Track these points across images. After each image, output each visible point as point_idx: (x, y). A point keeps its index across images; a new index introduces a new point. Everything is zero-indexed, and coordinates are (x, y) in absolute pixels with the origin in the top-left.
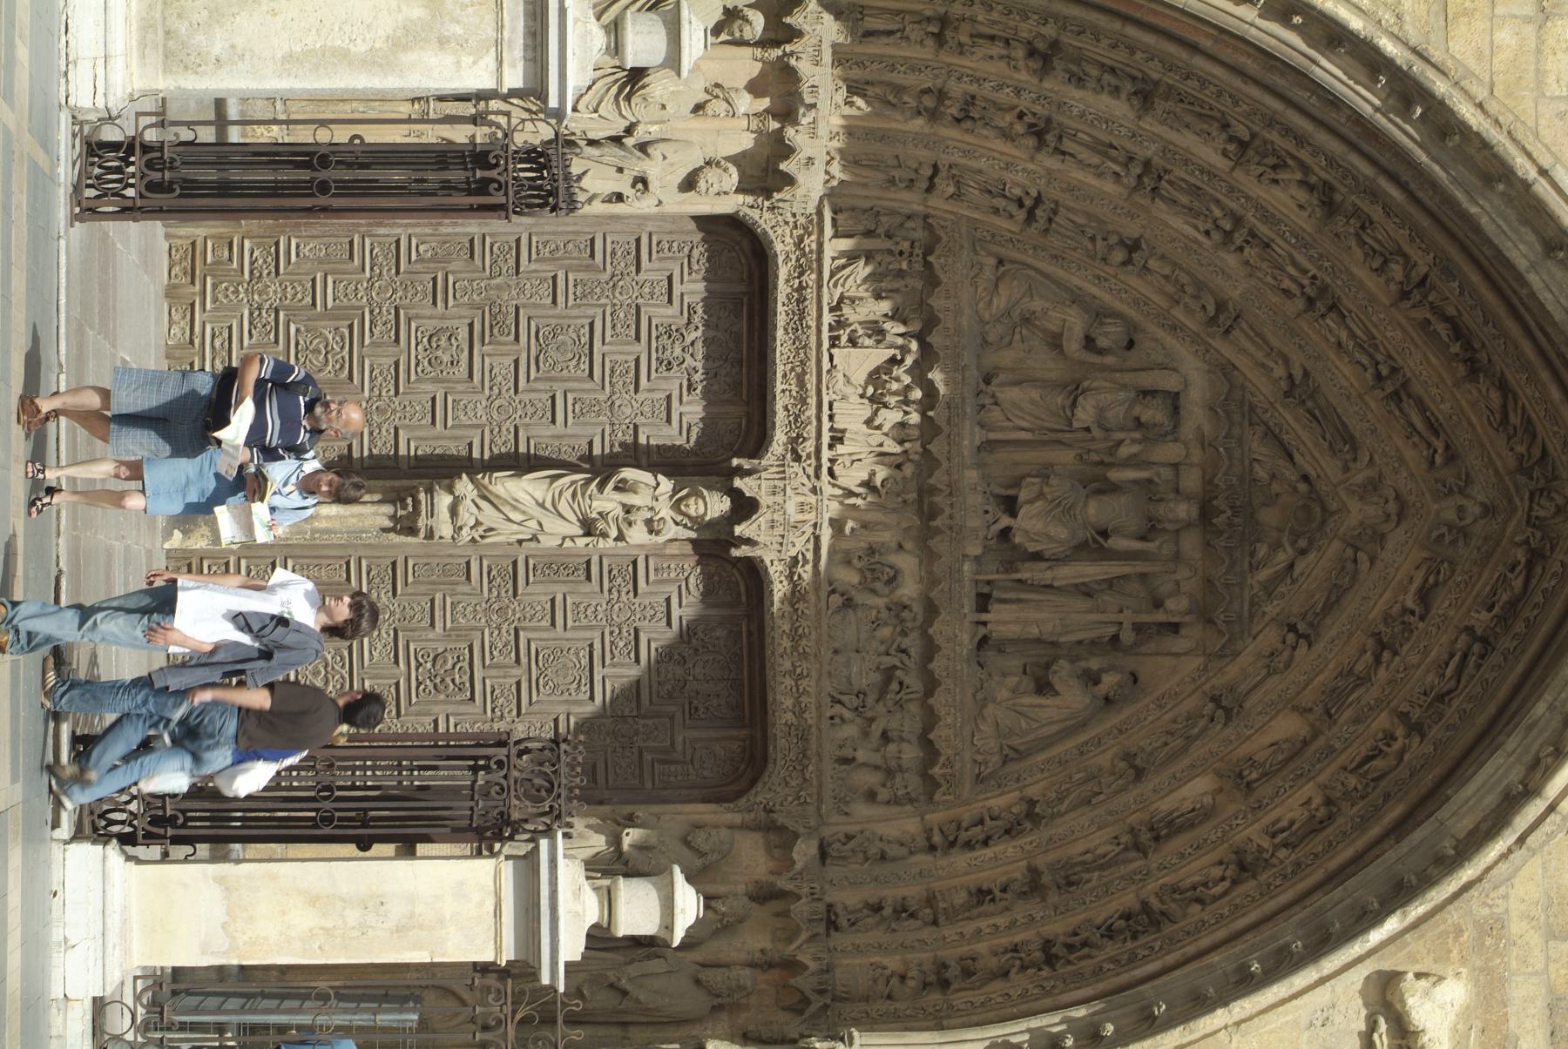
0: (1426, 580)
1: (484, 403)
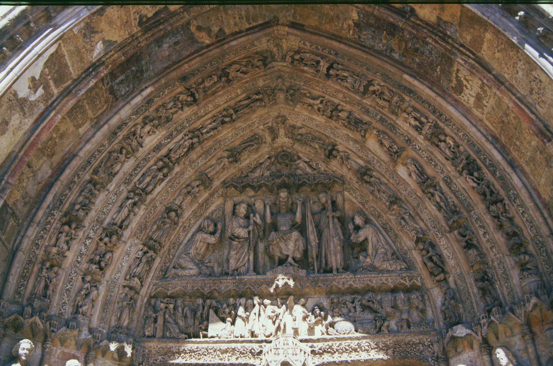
0: (308, 97)
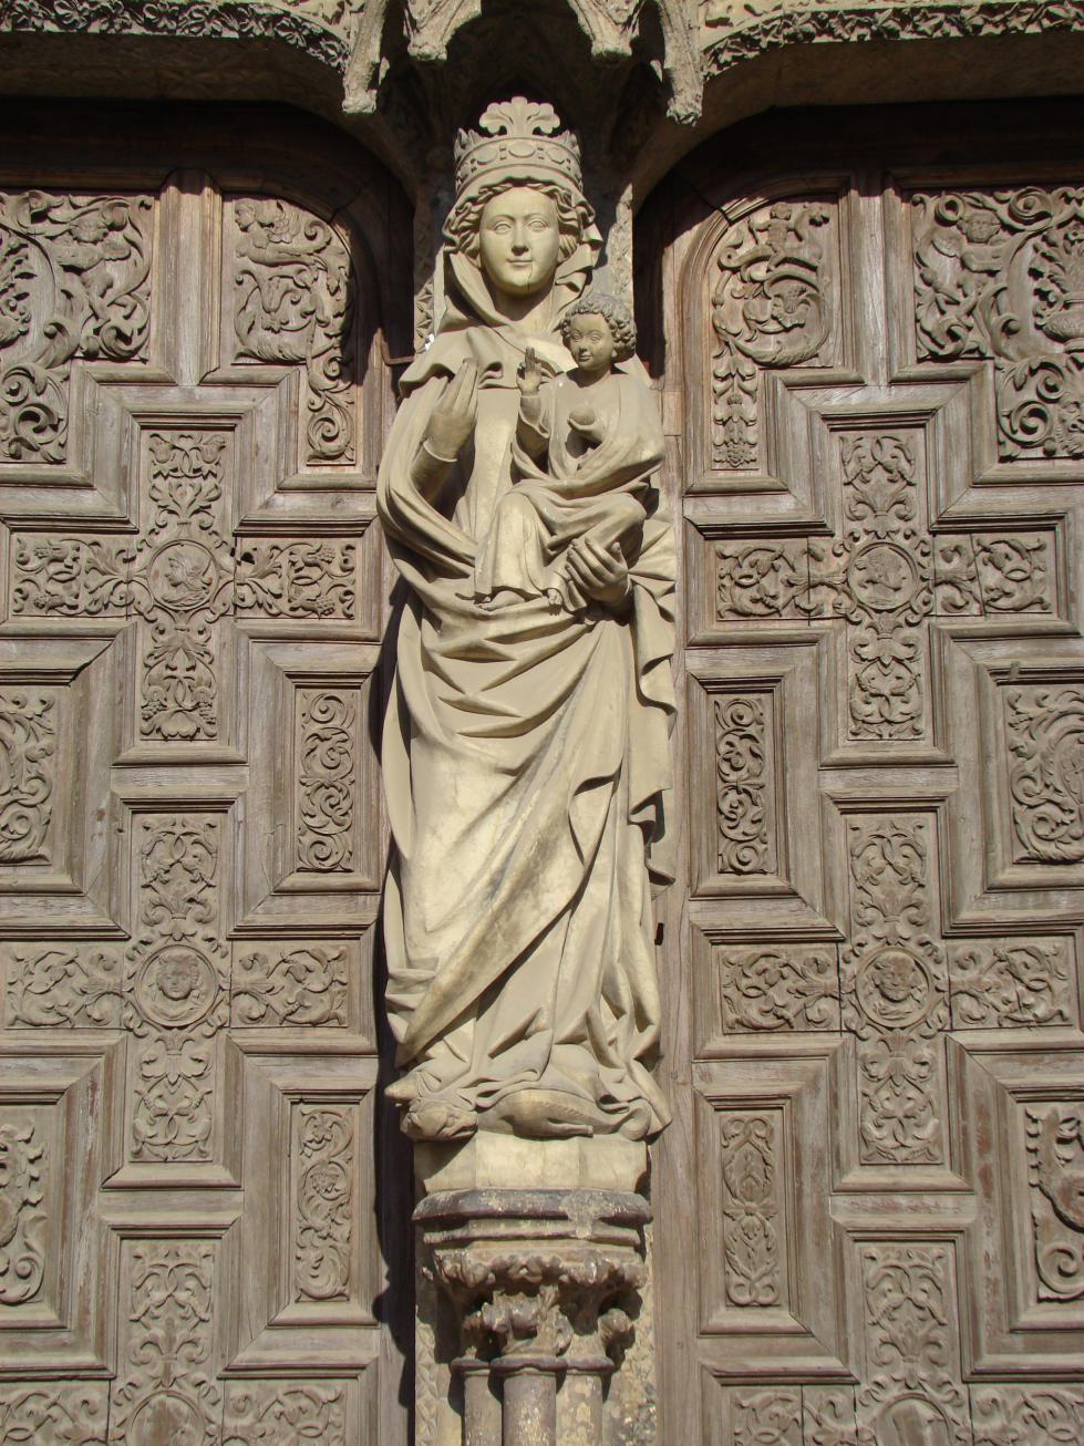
1: (146, 1049)
